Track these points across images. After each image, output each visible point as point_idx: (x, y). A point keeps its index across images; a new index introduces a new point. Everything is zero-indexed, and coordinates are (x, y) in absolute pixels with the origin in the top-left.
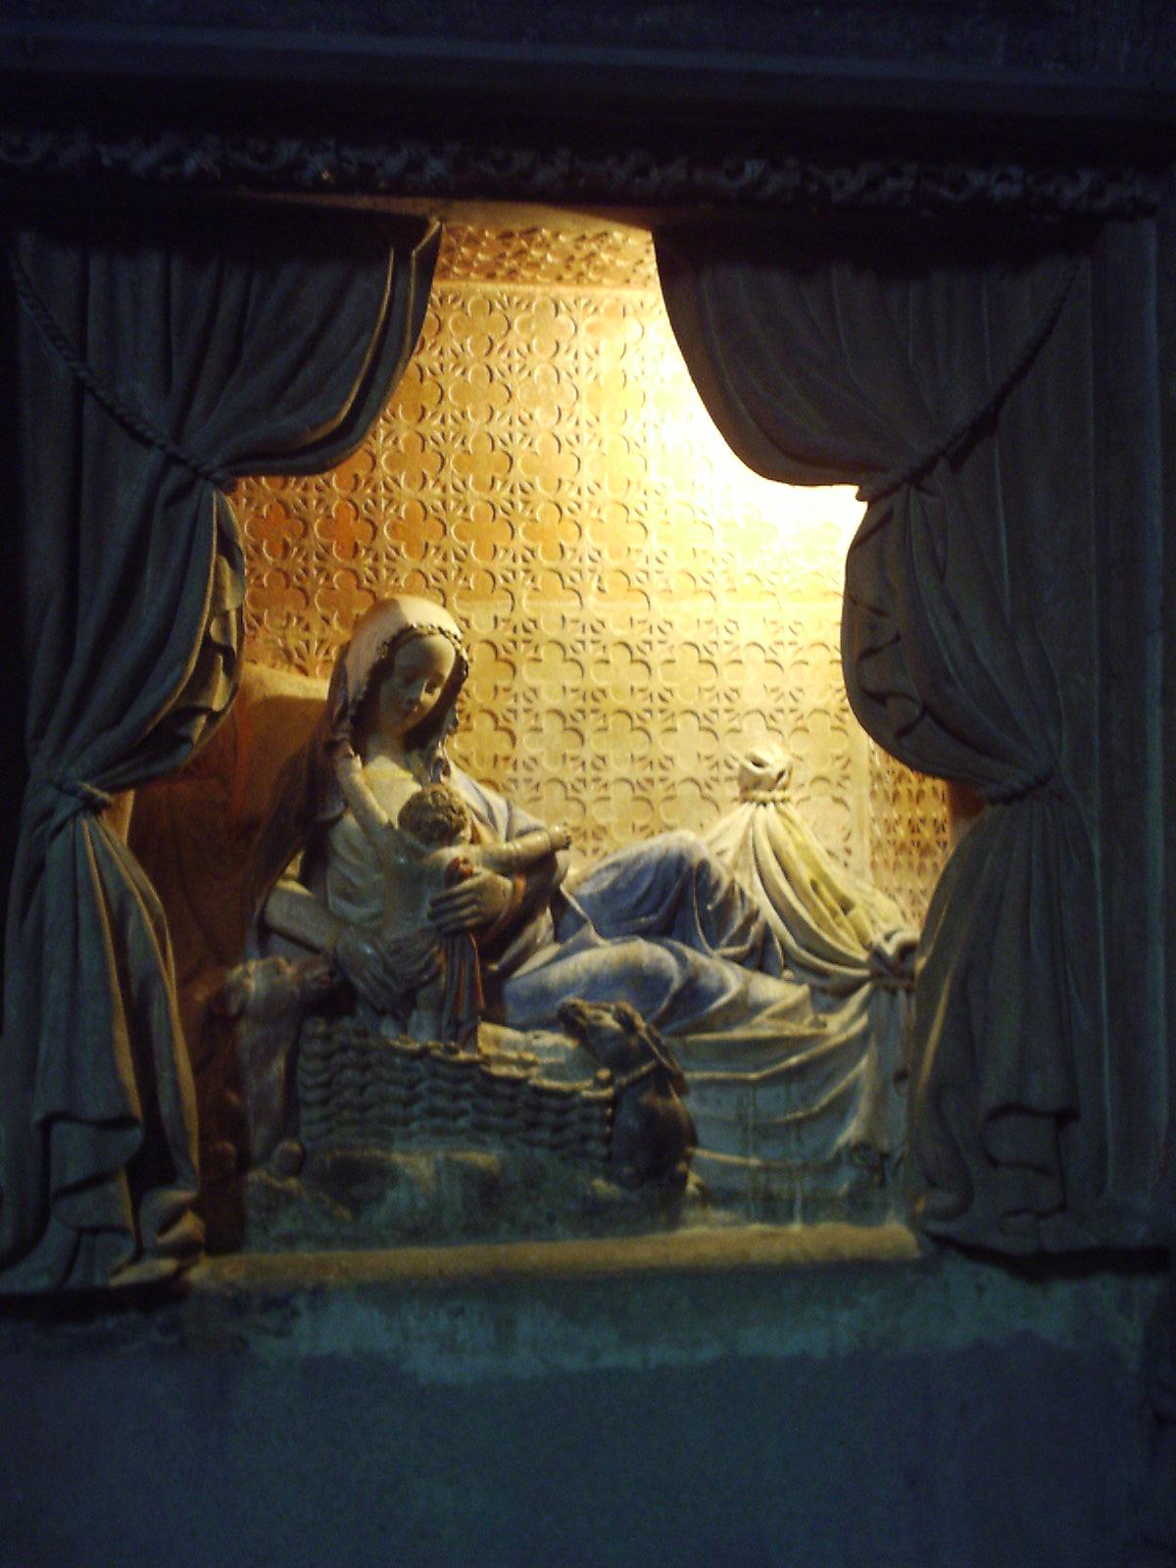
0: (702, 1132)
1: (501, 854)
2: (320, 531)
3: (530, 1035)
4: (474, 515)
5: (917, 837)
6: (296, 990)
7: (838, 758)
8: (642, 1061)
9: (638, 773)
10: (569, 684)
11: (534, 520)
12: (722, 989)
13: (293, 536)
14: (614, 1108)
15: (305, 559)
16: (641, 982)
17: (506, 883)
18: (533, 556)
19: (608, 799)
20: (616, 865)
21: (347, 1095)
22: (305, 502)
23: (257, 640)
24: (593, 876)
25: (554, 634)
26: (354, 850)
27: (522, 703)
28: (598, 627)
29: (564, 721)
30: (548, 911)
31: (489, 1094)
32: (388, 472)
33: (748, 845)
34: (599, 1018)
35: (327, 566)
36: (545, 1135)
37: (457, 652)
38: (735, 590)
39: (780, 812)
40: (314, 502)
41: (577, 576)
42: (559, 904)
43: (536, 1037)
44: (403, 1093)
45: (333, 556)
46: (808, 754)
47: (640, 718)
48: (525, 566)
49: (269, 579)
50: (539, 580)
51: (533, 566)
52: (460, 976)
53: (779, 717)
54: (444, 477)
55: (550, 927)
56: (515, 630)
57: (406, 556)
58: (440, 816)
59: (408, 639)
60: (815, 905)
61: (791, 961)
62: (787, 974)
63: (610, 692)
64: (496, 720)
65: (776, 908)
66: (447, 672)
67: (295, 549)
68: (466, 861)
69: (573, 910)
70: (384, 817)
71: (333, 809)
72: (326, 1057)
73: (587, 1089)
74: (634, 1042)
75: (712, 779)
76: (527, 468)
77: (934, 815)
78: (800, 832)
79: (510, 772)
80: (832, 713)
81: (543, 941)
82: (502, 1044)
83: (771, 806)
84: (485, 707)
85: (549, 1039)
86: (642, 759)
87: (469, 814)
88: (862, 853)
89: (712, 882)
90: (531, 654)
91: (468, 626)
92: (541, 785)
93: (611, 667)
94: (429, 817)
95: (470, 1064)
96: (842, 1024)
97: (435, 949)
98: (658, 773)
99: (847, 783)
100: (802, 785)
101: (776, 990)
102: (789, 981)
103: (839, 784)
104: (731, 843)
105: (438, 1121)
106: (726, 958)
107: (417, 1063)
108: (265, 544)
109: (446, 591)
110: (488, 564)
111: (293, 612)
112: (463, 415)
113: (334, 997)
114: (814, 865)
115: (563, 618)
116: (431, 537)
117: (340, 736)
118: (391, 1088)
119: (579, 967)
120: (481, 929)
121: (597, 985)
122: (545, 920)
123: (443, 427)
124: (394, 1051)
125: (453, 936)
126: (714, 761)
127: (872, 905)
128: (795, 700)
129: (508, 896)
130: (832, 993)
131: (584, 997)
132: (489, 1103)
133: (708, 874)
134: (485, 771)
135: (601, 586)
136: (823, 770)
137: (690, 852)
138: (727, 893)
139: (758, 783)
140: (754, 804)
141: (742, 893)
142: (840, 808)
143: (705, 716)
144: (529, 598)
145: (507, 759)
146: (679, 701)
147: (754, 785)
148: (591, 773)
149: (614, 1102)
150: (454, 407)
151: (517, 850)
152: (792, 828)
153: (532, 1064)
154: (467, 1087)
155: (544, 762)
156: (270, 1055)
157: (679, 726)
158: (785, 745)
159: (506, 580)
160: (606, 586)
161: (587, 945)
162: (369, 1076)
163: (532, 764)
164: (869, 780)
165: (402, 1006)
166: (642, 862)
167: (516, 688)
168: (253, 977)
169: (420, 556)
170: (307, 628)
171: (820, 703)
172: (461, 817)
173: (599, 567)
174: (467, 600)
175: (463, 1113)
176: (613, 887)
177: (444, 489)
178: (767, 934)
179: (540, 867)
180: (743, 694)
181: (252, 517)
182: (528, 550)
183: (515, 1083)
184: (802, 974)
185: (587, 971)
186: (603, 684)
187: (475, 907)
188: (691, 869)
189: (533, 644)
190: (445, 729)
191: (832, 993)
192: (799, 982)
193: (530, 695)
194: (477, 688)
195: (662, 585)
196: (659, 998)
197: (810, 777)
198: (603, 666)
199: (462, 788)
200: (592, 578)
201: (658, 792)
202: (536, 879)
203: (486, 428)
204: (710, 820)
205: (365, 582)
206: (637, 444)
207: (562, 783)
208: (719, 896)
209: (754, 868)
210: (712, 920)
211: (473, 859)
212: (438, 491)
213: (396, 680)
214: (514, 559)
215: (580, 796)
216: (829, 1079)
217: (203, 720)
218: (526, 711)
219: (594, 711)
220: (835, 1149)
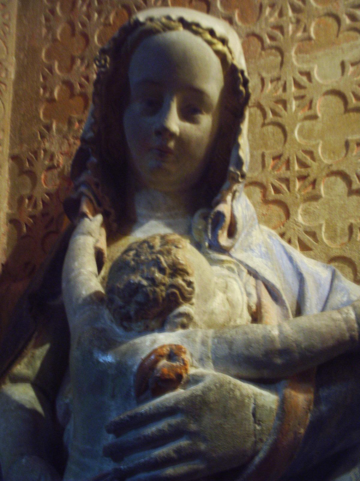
1: (248, 344)
17: (268, 398)
58: (136, 278)
66: (213, 86)
84: (334, 168)
109: (283, 48)
129: (271, 422)
134: (336, 249)
174: (307, 52)
181: (101, 27)
187: (183, 443)
194: (324, 148)
213: (137, 107)
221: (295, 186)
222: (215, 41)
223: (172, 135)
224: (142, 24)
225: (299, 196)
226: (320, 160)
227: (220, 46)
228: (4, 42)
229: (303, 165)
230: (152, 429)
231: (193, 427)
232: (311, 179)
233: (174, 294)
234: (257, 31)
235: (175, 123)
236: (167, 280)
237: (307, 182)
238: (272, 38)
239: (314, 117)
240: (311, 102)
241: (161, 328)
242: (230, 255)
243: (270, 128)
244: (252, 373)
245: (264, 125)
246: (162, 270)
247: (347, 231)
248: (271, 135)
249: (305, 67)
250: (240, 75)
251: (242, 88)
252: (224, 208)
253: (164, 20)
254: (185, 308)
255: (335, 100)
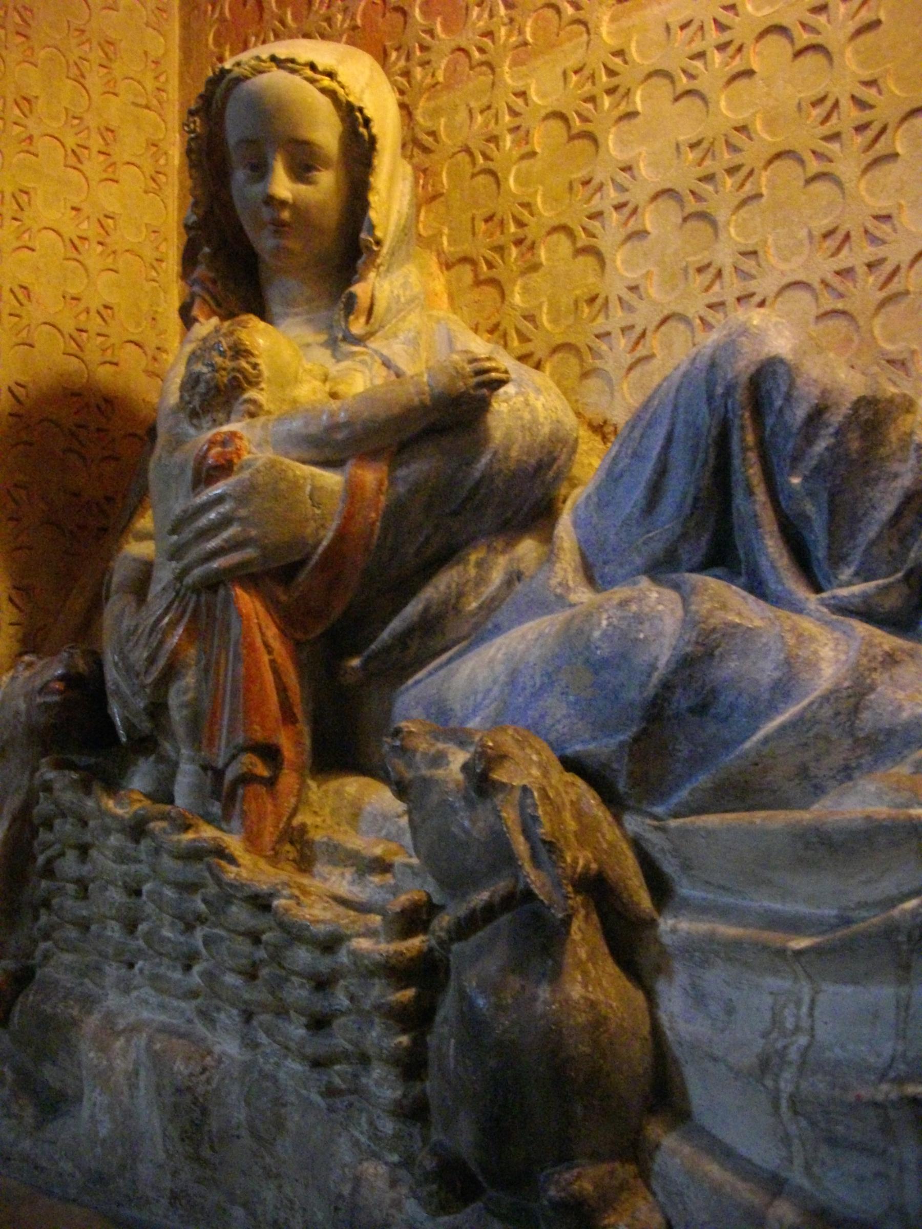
17: (332, 479)
36: (297, 1030)
57: (443, 36)
66: (327, 134)
73: (370, 933)
84: (556, 222)
93: (756, 78)
109: (494, 63)
144: (613, 19)
167: (599, 178)
174: (523, 63)
207: (682, 318)
213: (240, 175)
221: (510, 255)
222: (318, 77)
223: (283, 203)
224: (229, 71)
225: (515, 268)
226: (541, 215)
227: (326, 82)
228: (160, 115)
229: (520, 224)
230: (203, 522)
231: (243, 512)
232: (528, 242)
233: (235, 378)
234: (463, 45)
235: (282, 185)
236: (229, 364)
237: (524, 248)
238: (481, 50)
239: (533, 154)
240: (528, 133)
242: (365, 346)
243: (481, 179)
244: (312, 454)
245: (474, 176)
246: (222, 354)
247: (572, 307)
248: (481, 189)
249: (519, 85)
250: (358, 114)
251: (362, 130)
252: (360, 289)
253: (253, 62)
254: (252, 394)
255: (556, 126)
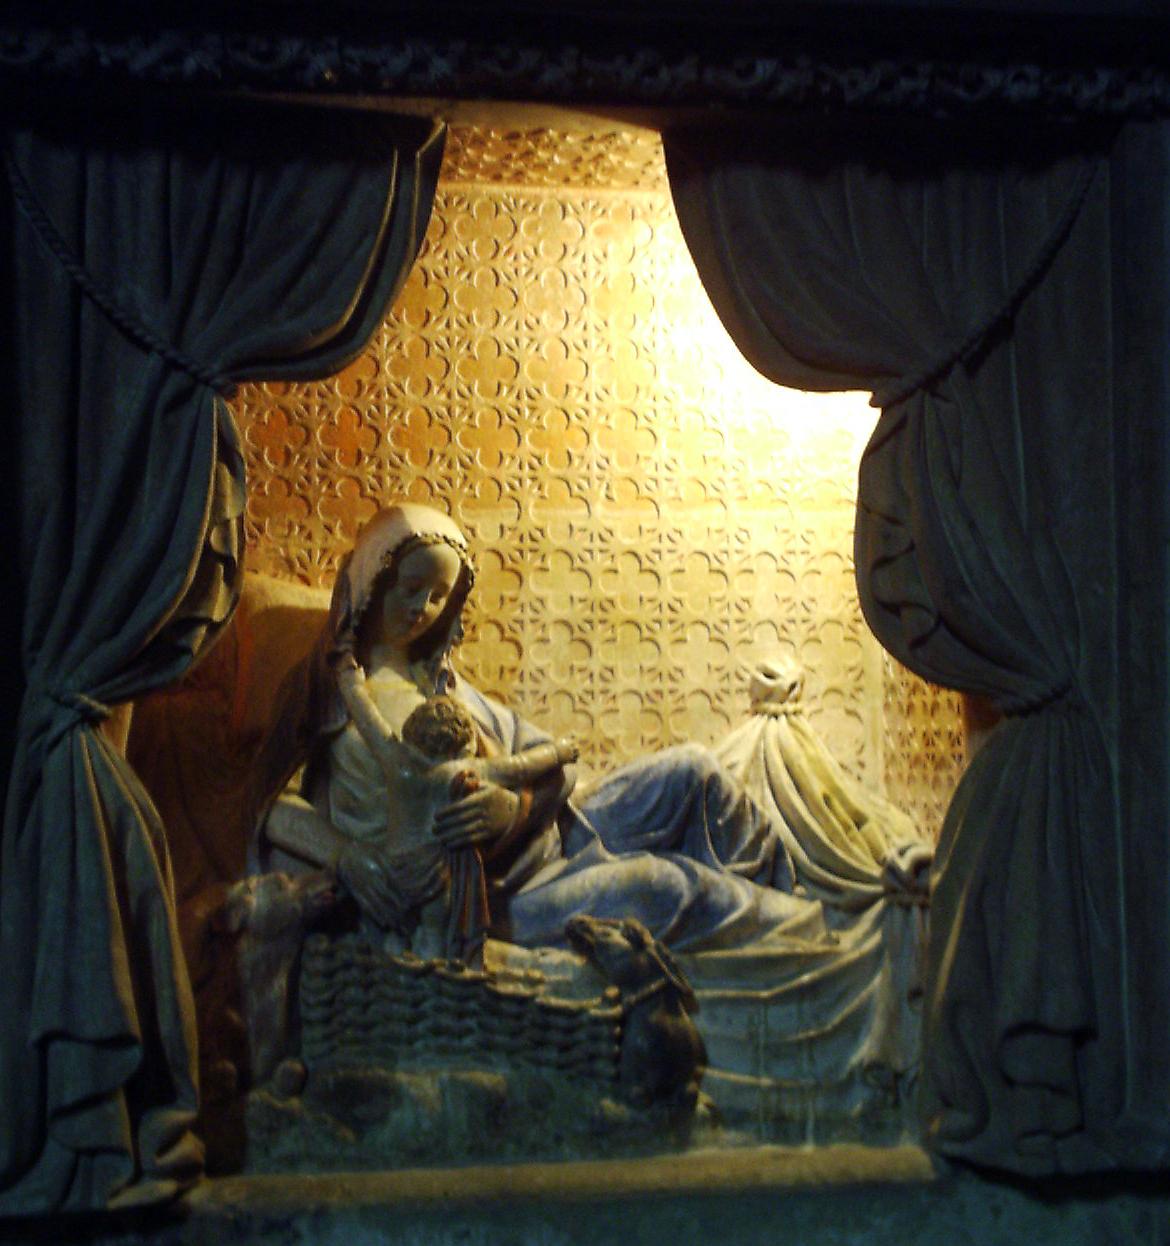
0: (712, 1052)
1: (507, 768)
2: (322, 437)
3: (537, 952)
4: (480, 421)
5: (932, 750)
6: (298, 906)
7: (851, 669)
8: (651, 978)
9: (647, 685)
10: (577, 594)
11: (541, 427)
12: (733, 905)
13: (295, 443)
14: (622, 1027)
15: (308, 466)
16: (650, 898)
17: (513, 797)
18: (540, 463)
19: (617, 711)
20: (624, 779)
21: (351, 1013)
22: (307, 408)
23: (258, 549)
24: (601, 790)
25: (562, 542)
26: (358, 764)
27: (529, 614)
28: (606, 535)
29: (572, 632)
30: (555, 825)
31: (495, 1013)
32: (392, 377)
33: (760, 759)
34: (607, 935)
35: (330, 474)
36: (552, 1054)
37: (463, 561)
38: (746, 498)
39: (792, 725)
40: (317, 409)
41: (584, 484)
42: (567, 818)
43: (543, 955)
44: (406, 1011)
45: (336, 464)
46: (820, 665)
47: (649, 629)
48: (532, 473)
49: (270, 489)
50: (546, 488)
51: (540, 473)
52: (465, 893)
53: (791, 627)
54: (449, 382)
55: (557, 842)
56: (521, 539)
57: (410, 463)
58: (445, 729)
59: (412, 547)
60: (827, 820)
61: (803, 876)
62: (799, 889)
63: (618, 602)
64: (502, 631)
65: (788, 822)
66: (452, 582)
67: (297, 457)
68: (471, 775)
69: (581, 824)
70: (388, 730)
71: (336, 721)
72: (329, 975)
73: (595, 1007)
74: (643, 959)
75: (722, 690)
76: (534, 373)
77: (949, 727)
78: (813, 745)
79: (516, 683)
80: (845, 624)
81: (550, 856)
82: (508, 961)
83: (783, 718)
84: (491, 618)
85: (556, 956)
86: (651, 670)
87: (475, 727)
88: (876, 766)
89: (723, 796)
90: (538, 563)
91: (474, 535)
92: (548, 697)
94: (434, 730)
95: (476, 982)
96: (855, 941)
97: (440, 864)
98: (667, 685)
99: (860, 696)
100: (815, 697)
101: (788, 906)
102: (801, 897)
103: (853, 696)
104: (742, 756)
105: (443, 1040)
106: (737, 873)
107: (422, 981)
108: (266, 451)
110: (494, 472)
111: (296, 521)
112: (469, 319)
113: (336, 914)
114: (827, 779)
115: (571, 527)
116: (435, 443)
117: (342, 648)
118: (395, 1007)
119: (587, 884)
120: (487, 844)
121: (605, 902)
122: (552, 834)
123: (448, 332)
124: (399, 968)
125: (457, 850)
126: (724, 672)
127: (886, 820)
128: (808, 610)
129: (515, 809)
130: (845, 909)
131: (592, 914)
132: (495, 1022)
133: (719, 788)
134: (491, 683)
135: (610, 494)
136: (836, 682)
137: (700, 766)
138: (738, 807)
139: (769, 695)
140: (766, 717)
141: (753, 807)
142: (853, 720)
143: (716, 627)
144: (536, 506)
145: (513, 670)
146: (690, 611)
147: (765, 697)
148: (599, 685)
149: (622, 1021)
150: (459, 312)
151: (523, 763)
152: (803, 740)
153: (540, 982)
154: (473, 1005)
155: (551, 673)
156: (271, 974)
157: (689, 637)
158: (797, 656)
159: (512, 487)
160: (614, 494)
161: (595, 860)
162: (372, 994)
163: (539, 676)
164: (882, 691)
165: (406, 923)
166: (651, 775)
167: (523, 598)
168: (254, 893)
169: (425, 464)
170: (309, 537)
171: (833, 613)
172: (467, 730)
173: (607, 475)
174: (473, 508)
175: (469, 1031)
176: (623, 798)
177: (449, 395)
178: (779, 849)
179: (545, 783)
180: (755, 603)
181: (254, 424)
182: (535, 457)
183: (522, 1001)
184: (814, 890)
185: (595, 887)
186: (611, 594)
187: (480, 822)
188: (701, 782)
189: (540, 553)
190: (450, 640)
191: (845, 909)
192: (811, 898)
193: (537, 605)
194: (483, 598)
195: (672, 493)
196: (670, 914)
197: (823, 688)
198: (611, 576)
199: (467, 700)
200: (600, 486)
201: (667, 704)
202: (543, 793)
203: (492, 333)
204: (721, 732)
205: (369, 490)
206: (646, 349)
207: (569, 695)
208: (730, 810)
209: (766, 782)
210: (723, 834)
211: (479, 773)
212: (443, 397)
213: (400, 590)
214: (521, 467)
215: (587, 708)
216: (842, 997)
217: (203, 630)
218: (533, 621)
219: (603, 622)
220: (848, 1068)
234: (428, 477)
241: (455, 757)
246: (460, 724)
